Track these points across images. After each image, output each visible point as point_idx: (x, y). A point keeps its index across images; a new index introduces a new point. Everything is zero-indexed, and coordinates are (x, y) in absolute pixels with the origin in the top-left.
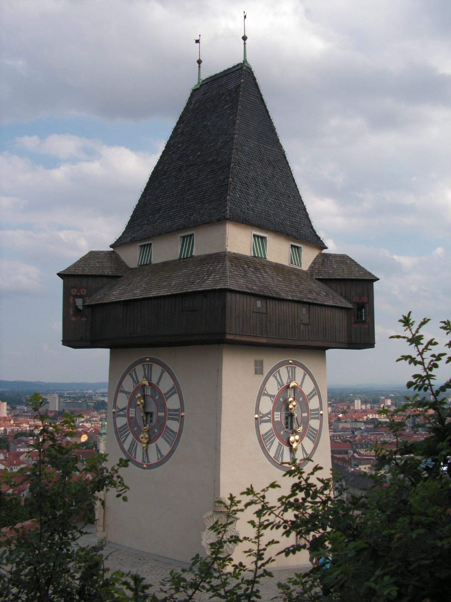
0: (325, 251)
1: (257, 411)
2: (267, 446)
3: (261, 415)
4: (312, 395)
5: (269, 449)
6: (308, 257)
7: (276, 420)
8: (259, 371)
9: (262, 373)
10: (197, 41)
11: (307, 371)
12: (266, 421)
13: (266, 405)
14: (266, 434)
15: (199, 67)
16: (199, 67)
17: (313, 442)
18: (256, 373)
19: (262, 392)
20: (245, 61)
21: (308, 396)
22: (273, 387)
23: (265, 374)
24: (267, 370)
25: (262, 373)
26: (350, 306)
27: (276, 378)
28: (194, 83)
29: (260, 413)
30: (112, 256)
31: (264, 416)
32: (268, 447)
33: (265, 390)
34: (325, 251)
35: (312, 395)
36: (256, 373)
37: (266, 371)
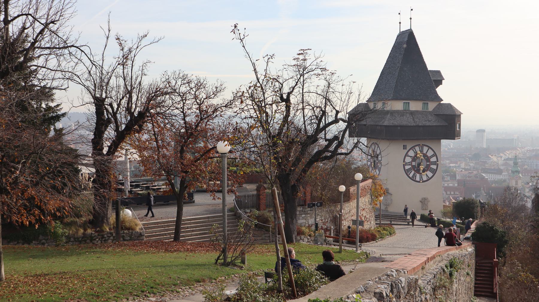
0: (442, 102)
1: (404, 161)
6: (432, 106)
9: (406, 149)
11: (429, 148)
13: (408, 160)
19: (406, 155)
20: (411, 29)
22: (411, 153)
23: (408, 150)
25: (406, 149)
26: (447, 124)
28: (398, 33)
30: (366, 105)
34: (442, 102)
37: (408, 149)
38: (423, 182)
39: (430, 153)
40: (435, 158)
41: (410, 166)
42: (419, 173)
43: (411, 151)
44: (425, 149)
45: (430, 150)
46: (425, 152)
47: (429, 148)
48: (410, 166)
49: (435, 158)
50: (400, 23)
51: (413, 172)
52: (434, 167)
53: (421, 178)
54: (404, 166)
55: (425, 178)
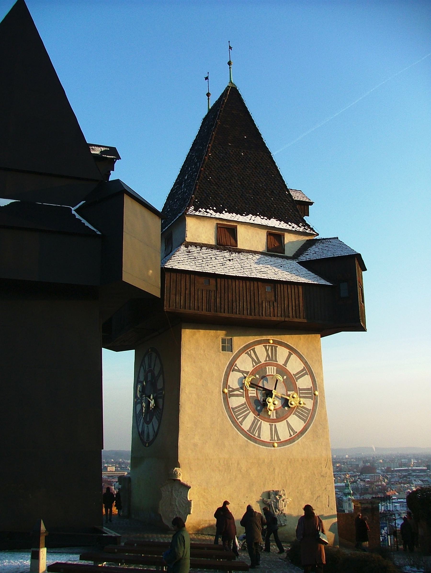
2: (238, 419)
3: (230, 389)
4: (301, 374)
5: (241, 422)
7: (250, 395)
8: (227, 346)
10: (207, 78)
12: (237, 395)
14: (236, 408)
15: (208, 99)
16: (208, 99)
17: (305, 421)
18: (224, 349)
19: (231, 367)
21: (295, 375)
22: (245, 364)
23: (236, 351)
24: (237, 347)
27: (250, 355)
29: (229, 387)
31: (234, 390)
32: (240, 420)
33: (236, 366)
35: (301, 374)
36: (224, 349)
38: (282, 444)
39: (295, 366)
40: (307, 378)
41: (242, 400)
42: (268, 419)
43: (244, 356)
44: (282, 353)
45: (294, 357)
46: (281, 361)
47: (292, 350)
48: (242, 400)
49: (307, 378)
50: (208, 95)
51: (251, 416)
52: (309, 404)
53: (274, 432)
54: (226, 397)
55: (284, 435)
